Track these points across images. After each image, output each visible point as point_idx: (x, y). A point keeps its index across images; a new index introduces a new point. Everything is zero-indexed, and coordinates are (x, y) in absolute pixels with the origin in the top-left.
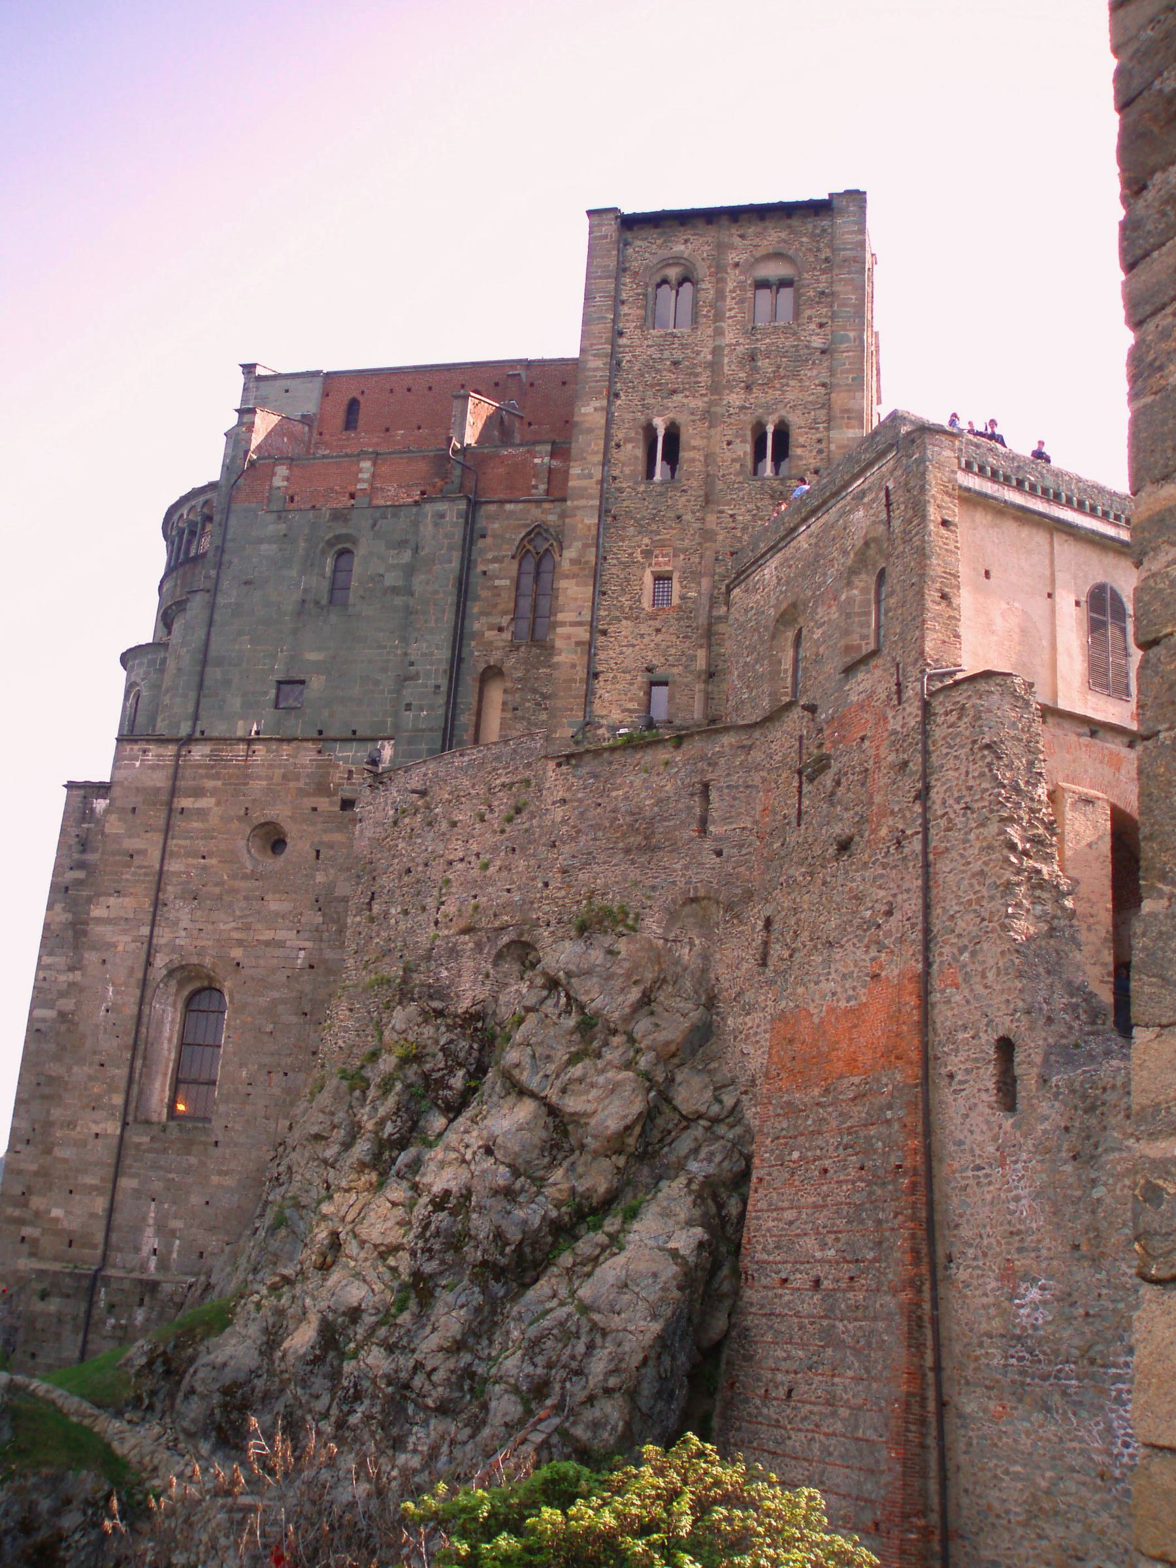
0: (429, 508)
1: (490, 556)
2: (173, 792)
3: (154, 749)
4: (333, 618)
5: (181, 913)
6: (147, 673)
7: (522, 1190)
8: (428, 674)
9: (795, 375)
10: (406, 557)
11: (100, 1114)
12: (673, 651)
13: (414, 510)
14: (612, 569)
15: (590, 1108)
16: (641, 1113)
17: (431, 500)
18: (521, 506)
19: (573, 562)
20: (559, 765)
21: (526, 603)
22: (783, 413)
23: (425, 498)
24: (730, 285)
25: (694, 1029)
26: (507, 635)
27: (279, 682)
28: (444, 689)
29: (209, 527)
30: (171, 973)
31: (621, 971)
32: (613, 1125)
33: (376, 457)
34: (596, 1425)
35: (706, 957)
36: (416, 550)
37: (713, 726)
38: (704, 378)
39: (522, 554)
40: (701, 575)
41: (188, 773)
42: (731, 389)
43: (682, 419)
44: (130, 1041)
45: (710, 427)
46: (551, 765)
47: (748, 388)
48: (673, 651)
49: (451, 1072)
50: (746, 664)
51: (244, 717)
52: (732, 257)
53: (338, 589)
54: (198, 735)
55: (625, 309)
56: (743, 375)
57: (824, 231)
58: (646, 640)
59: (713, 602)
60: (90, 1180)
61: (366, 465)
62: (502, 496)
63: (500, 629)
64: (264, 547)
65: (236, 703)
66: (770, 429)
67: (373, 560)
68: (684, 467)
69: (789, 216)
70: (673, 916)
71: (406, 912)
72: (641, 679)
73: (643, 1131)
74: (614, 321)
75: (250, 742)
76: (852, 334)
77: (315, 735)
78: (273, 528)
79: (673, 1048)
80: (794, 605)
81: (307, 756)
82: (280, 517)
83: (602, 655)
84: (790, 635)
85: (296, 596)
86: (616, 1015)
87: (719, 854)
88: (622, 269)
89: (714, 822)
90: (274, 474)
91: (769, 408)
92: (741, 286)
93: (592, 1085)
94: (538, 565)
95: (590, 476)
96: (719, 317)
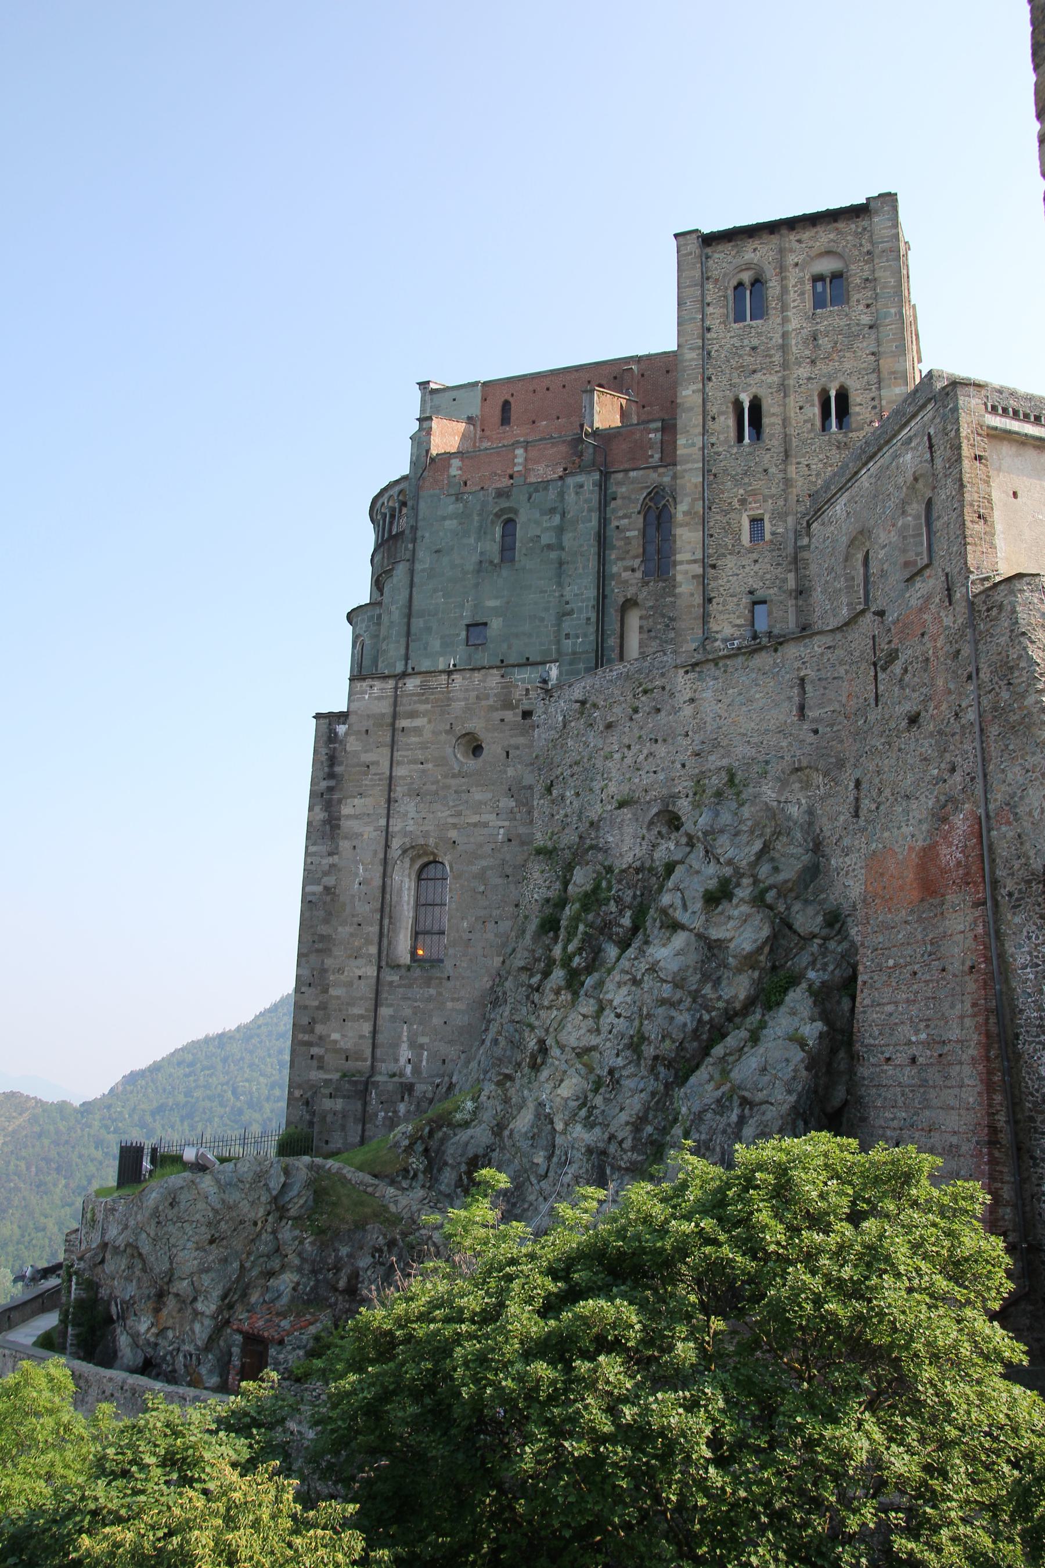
0: (570, 481)
1: (620, 513)
4: (505, 573)
6: (368, 627)
7: (680, 1001)
8: (580, 609)
9: (850, 348)
10: (557, 519)
12: (768, 576)
13: (560, 483)
14: (716, 518)
15: (728, 935)
17: (572, 474)
18: (641, 472)
19: (685, 513)
20: (687, 672)
21: (652, 549)
22: (842, 379)
23: (567, 473)
24: (792, 281)
25: (806, 869)
26: (639, 574)
27: (468, 626)
28: (593, 620)
29: (404, 510)
31: (745, 828)
32: (748, 947)
33: (527, 445)
35: (810, 812)
36: (563, 515)
37: (805, 631)
38: (777, 358)
39: (645, 511)
40: (787, 514)
42: (799, 364)
43: (762, 392)
45: (785, 397)
46: (681, 671)
47: (813, 362)
48: (768, 576)
49: (621, 913)
50: (827, 582)
51: (443, 654)
52: (792, 259)
53: (507, 549)
54: (410, 670)
55: (710, 310)
56: (807, 352)
57: (865, 229)
58: (747, 570)
59: (797, 535)
61: (520, 452)
62: (627, 466)
63: (633, 570)
64: (447, 523)
65: (436, 644)
66: (833, 394)
67: (532, 524)
68: (767, 430)
69: (835, 221)
70: (783, 783)
71: (578, 794)
72: (746, 600)
73: (771, 950)
74: (703, 320)
75: (449, 673)
76: (893, 311)
77: (499, 664)
78: (451, 507)
79: (790, 885)
80: (861, 532)
81: (494, 680)
82: (457, 499)
83: (713, 584)
84: (860, 556)
85: (475, 558)
86: (744, 862)
87: (816, 732)
88: (705, 278)
89: (810, 708)
90: (450, 466)
91: (831, 377)
92: (801, 281)
93: (729, 918)
94: (659, 517)
95: (693, 445)
96: (784, 308)
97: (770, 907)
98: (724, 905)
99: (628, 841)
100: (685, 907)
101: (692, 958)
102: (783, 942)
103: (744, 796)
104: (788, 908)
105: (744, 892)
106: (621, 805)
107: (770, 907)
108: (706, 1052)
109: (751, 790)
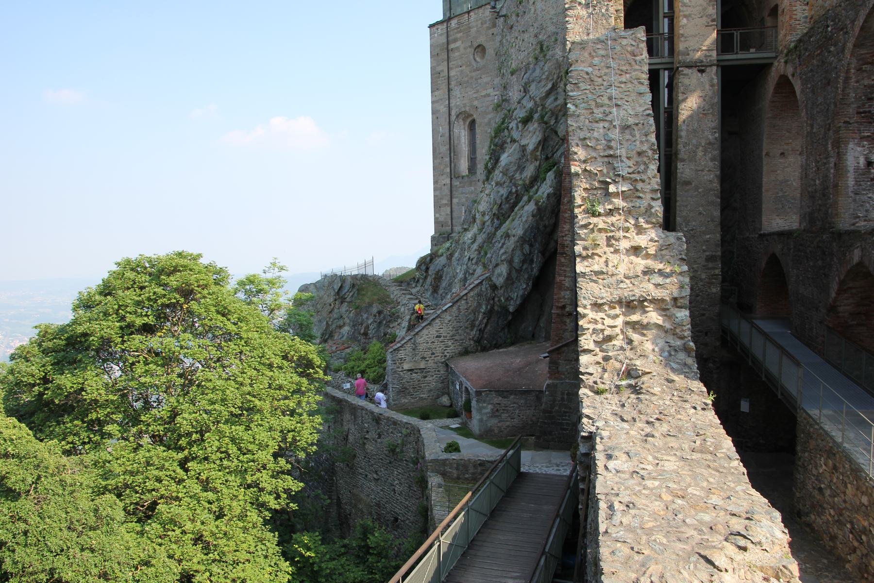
2: (448, 43)
3: (440, 27)
5: (457, 92)
7: (504, 182)
11: (445, 176)
16: (540, 141)
30: (457, 116)
34: (499, 275)
41: (451, 33)
44: (448, 146)
60: (444, 202)
75: (468, 12)
79: (559, 107)
97: (546, 123)
98: (529, 124)
99: (516, 94)
100: (518, 128)
101: (516, 156)
102: (551, 143)
103: (547, 57)
104: (557, 122)
105: (536, 116)
106: (512, 73)
107: (546, 123)
108: (512, 209)
109: (550, 53)
